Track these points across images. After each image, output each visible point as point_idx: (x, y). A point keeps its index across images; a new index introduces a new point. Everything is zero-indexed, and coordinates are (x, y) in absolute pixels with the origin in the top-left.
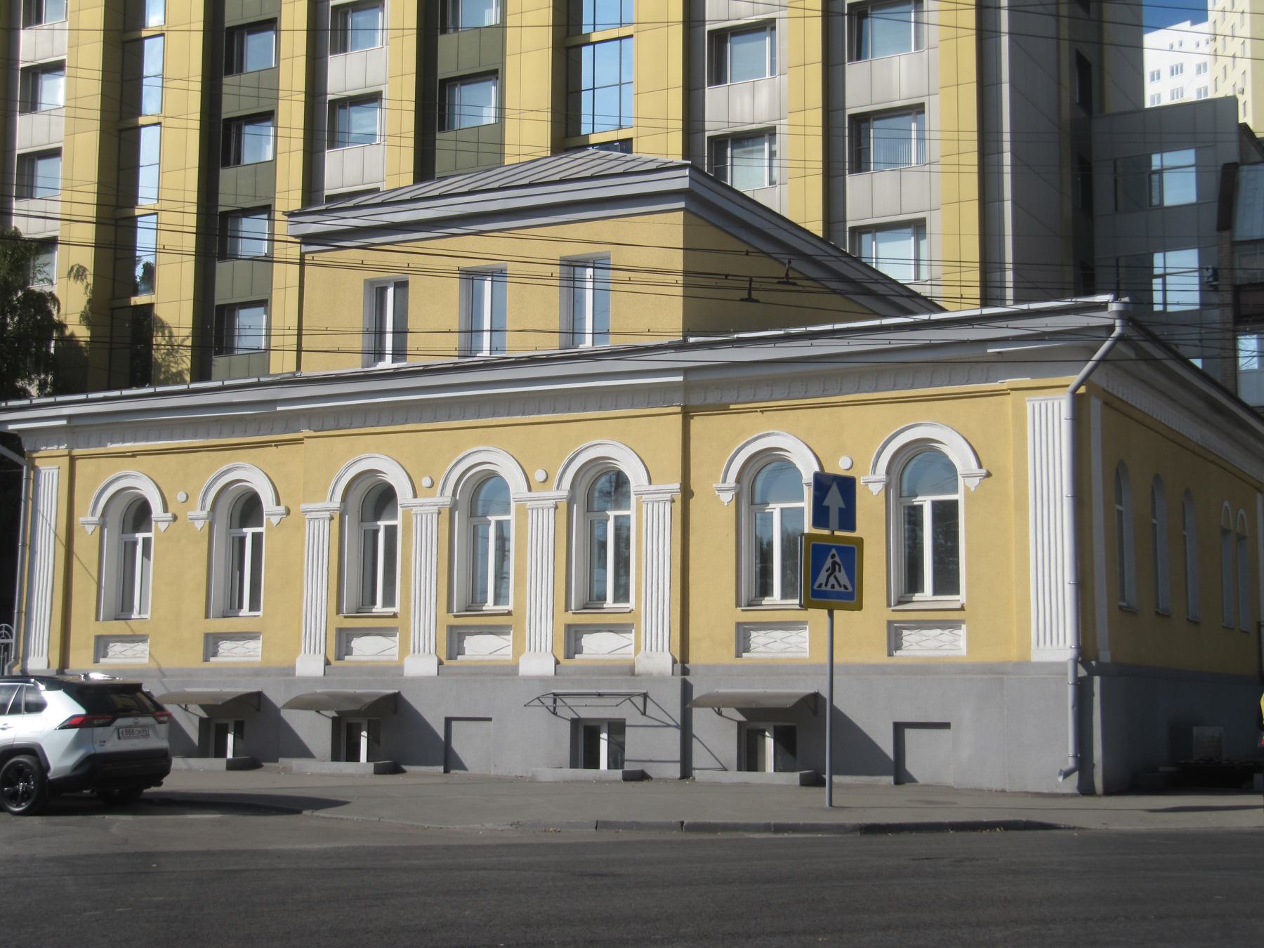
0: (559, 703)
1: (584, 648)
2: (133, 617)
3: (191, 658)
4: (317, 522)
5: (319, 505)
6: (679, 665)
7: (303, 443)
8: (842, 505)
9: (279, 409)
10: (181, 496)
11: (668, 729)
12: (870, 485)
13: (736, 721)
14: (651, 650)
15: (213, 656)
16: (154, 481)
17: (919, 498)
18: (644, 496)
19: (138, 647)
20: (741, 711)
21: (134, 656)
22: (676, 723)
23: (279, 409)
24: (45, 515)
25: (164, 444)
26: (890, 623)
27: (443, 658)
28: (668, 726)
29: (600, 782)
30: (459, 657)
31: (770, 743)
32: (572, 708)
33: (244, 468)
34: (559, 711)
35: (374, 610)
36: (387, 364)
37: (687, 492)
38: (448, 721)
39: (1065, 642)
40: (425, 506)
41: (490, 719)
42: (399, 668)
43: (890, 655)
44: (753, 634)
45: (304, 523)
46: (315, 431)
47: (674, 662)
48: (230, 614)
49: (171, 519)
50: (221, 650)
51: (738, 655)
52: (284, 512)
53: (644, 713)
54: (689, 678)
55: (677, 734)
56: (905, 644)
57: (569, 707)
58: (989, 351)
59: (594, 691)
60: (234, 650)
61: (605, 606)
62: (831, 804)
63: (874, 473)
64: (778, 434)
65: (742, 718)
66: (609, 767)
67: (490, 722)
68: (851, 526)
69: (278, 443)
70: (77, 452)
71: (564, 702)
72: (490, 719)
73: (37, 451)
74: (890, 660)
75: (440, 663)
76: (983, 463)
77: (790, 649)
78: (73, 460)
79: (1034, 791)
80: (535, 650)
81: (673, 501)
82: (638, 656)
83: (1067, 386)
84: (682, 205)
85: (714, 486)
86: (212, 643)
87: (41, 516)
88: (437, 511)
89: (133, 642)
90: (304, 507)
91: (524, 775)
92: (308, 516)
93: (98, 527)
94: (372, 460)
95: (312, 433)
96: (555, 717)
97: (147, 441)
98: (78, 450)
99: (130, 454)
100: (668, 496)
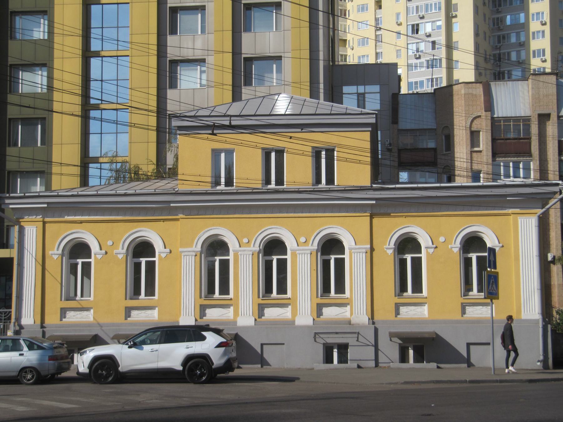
0: (317, 336)
1: (323, 313)
2: (77, 299)
3: (120, 318)
4: (188, 257)
5: (189, 249)
6: (371, 321)
7: (179, 221)
8: (494, 260)
9: (171, 205)
10: (110, 243)
11: (369, 347)
12: (453, 249)
13: (398, 343)
14: (361, 314)
15: (129, 317)
16: (162, 238)
17: (471, 254)
18: (353, 250)
19: (84, 313)
20: (400, 339)
21: (82, 318)
22: (372, 344)
23: (171, 205)
24: (29, 250)
25: (115, 218)
26: (462, 303)
27: (257, 318)
28: (369, 345)
29: (336, 369)
30: (321, 317)
31: (411, 352)
32: (324, 339)
33: (146, 231)
34: (317, 340)
35: (214, 297)
36: (222, 187)
37: (372, 249)
38: (262, 345)
39: (535, 311)
40: (246, 251)
41: (284, 344)
42: (235, 322)
43: (462, 316)
44: (401, 308)
45: (181, 257)
46: (186, 216)
47: (369, 319)
48: (133, 298)
49: (105, 253)
50: (132, 315)
51: (396, 316)
52: (169, 251)
53: (358, 340)
54: (377, 326)
55: (373, 348)
56: (467, 312)
57: (322, 338)
58: (508, 198)
59: (334, 331)
60: (139, 315)
61: (330, 295)
62: (494, 373)
63: (455, 244)
64: (412, 227)
65: (401, 342)
66: (338, 363)
67: (284, 345)
68: (495, 268)
69: (164, 220)
70: (47, 219)
71: (319, 336)
72: (284, 344)
73: (23, 218)
74: (462, 318)
75: (255, 320)
76: (500, 242)
77: (418, 314)
78: (44, 223)
79: (526, 368)
80: (242, 315)
81: (366, 252)
82: (352, 316)
83: (536, 213)
84: (370, 129)
85: (385, 247)
86: (128, 311)
87: (26, 251)
88: (252, 254)
89: (81, 311)
90: (180, 250)
91: (301, 367)
92: (183, 254)
93: (60, 256)
94: (217, 230)
95: (184, 217)
96: (316, 343)
97: (89, 216)
98: (47, 219)
99: (80, 222)
100: (364, 250)
